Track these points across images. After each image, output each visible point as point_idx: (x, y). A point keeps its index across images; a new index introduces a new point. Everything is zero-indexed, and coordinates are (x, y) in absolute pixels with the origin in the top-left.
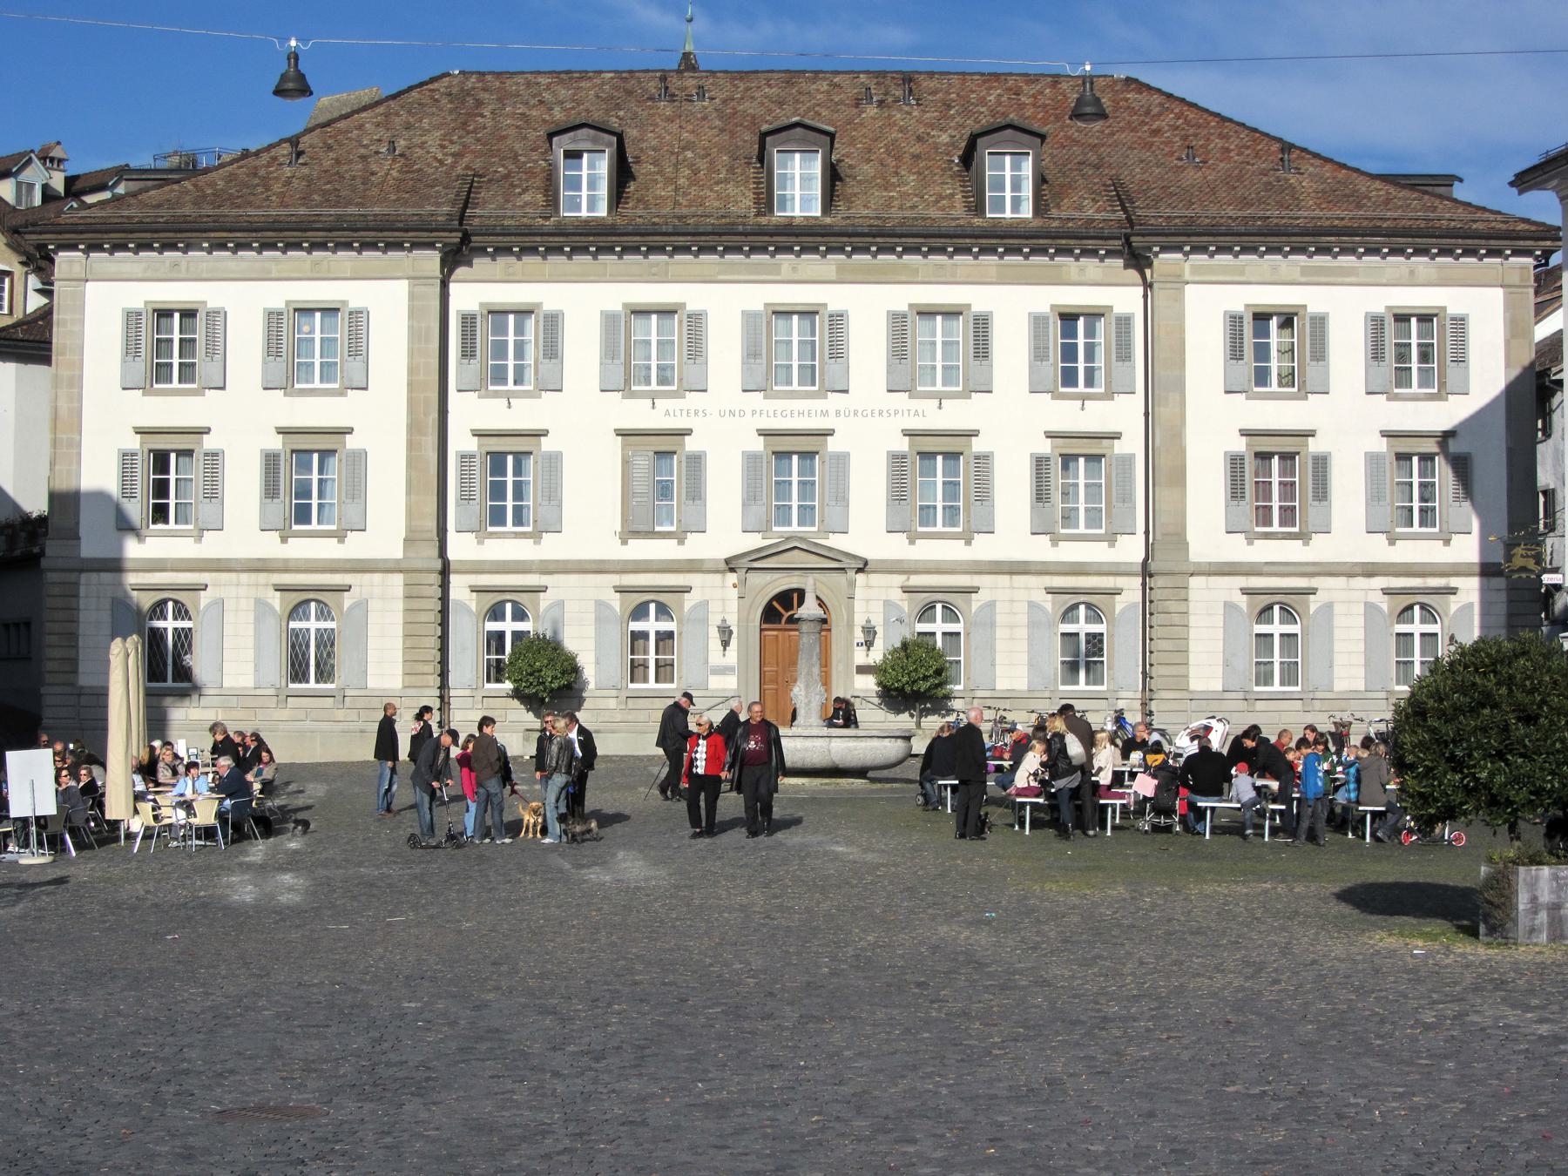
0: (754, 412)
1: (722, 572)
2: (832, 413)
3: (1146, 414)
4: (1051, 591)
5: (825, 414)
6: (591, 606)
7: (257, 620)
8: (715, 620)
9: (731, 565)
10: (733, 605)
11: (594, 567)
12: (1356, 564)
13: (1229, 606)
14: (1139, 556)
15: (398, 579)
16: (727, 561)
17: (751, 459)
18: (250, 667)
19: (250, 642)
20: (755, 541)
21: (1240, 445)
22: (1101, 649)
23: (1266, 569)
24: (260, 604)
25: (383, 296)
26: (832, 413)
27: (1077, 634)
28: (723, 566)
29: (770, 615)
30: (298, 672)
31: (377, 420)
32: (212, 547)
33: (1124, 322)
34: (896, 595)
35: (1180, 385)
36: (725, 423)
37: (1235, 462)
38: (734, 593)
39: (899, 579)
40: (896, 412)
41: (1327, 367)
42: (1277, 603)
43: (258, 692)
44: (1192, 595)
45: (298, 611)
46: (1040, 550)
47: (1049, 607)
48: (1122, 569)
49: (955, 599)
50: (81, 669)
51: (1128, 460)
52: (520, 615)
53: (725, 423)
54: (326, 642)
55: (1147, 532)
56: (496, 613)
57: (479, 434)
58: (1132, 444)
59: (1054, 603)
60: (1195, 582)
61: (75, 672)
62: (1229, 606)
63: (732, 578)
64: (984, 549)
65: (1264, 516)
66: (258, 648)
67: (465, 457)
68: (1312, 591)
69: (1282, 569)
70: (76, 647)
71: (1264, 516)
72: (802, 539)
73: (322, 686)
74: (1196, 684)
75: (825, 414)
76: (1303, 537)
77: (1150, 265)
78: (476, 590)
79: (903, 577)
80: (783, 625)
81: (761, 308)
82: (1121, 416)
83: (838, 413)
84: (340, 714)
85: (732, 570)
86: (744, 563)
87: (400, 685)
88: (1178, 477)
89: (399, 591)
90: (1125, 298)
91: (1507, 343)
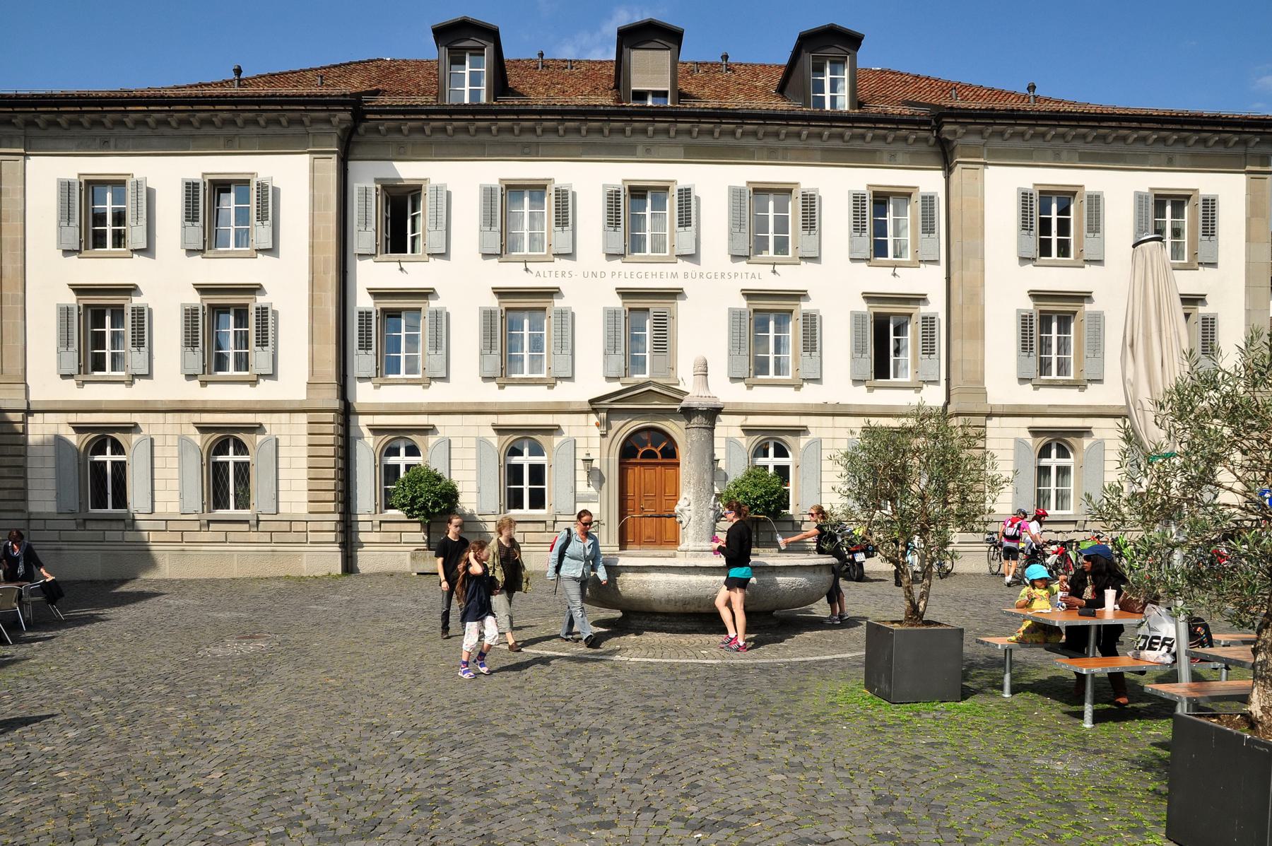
0: (613, 274)
1: (587, 412)
2: (681, 275)
3: (948, 279)
5: (675, 275)
6: (473, 443)
7: (181, 454)
8: (581, 455)
9: (595, 405)
10: (596, 441)
11: (475, 408)
13: (1019, 442)
14: (943, 400)
15: (303, 418)
16: (591, 402)
17: (612, 315)
18: (176, 496)
19: (176, 474)
20: (616, 386)
21: (1029, 305)
24: (183, 439)
25: (293, 177)
26: (681, 275)
28: (587, 407)
29: (628, 452)
30: (219, 500)
31: (287, 282)
32: (141, 391)
33: (928, 201)
34: (738, 433)
35: (979, 253)
36: (590, 284)
37: (1025, 321)
38: (597, 432)
39: (739, 420)
40: (736, 275)
42: (1057, 441)
43: (184, 517)
45: (221, 448)
46: (861, 397)
49: (788, 439)
50: (30, 498)
52: (413, 451)
53: (590, 284)
54: (243, 471)
55: (948, 380)
56: (515, 451)
57: (377, 294)
58: (936, 306)
61: (25, 500)
62: (1019, 442)
63: (593, 418)
64: (810, 395)
65: (1044, 367)
66: (182, 479)
67: (365, 316)
70: (25, 478)
71: (1044, 367)
72: (655, 384)
73: (241, 512)
75: (675, 275)
76: (1079, 385)
77: (952, 151)
78: (376, 431)
79: (743, 417)
80: (638, 460)
81: (620, 183)
82: (927, 281)
83: (686, 275)
84: (254, 536)
85: (596, 411)
86: (606, 404)
87: (306, 511)
88: (977, 332)
89: (304, 429)
90: (929, 181)
91: (1248, 220)
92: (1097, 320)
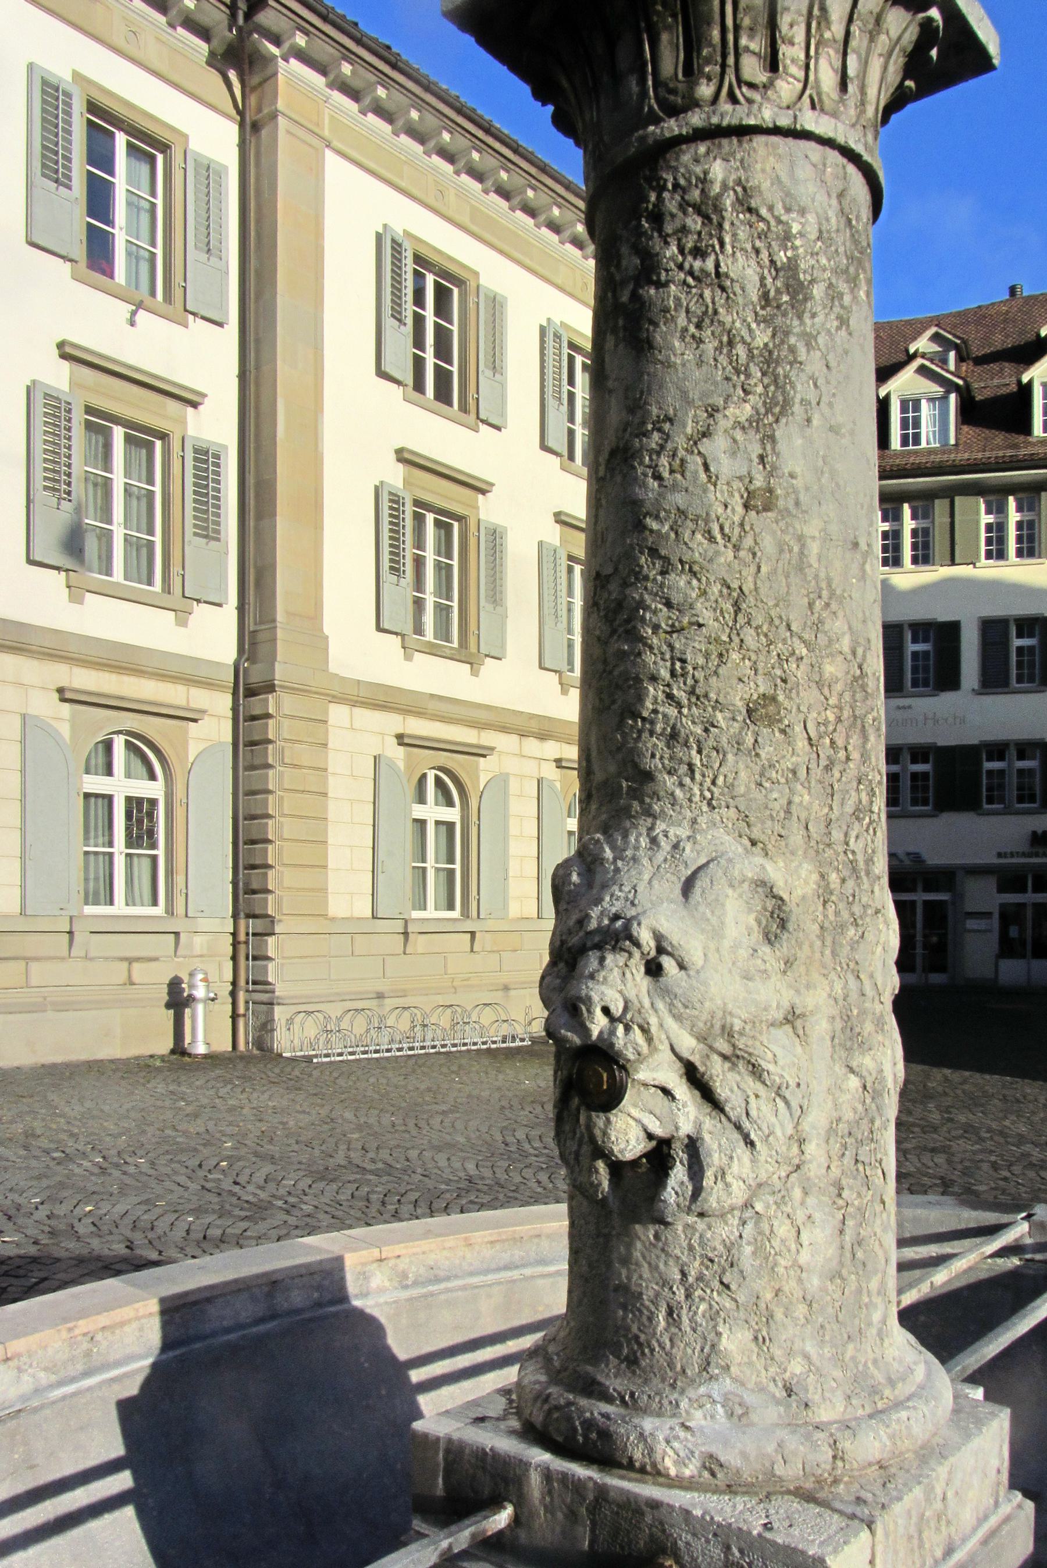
3: (243, 376)
4: (63, 694)
12: (532, 716)
22: (151, 833)
23: (432, 706)
27: (109, 799)
41: (503, 385)
44: (335, 739)
47: (65, 730)
48: (203, 672)
51: (206, 458)
59: (73, 721)
60: (338, 714)
68: (480, 752)
69: (444, 707)
74: (337, 907)
92: (496, 537)
